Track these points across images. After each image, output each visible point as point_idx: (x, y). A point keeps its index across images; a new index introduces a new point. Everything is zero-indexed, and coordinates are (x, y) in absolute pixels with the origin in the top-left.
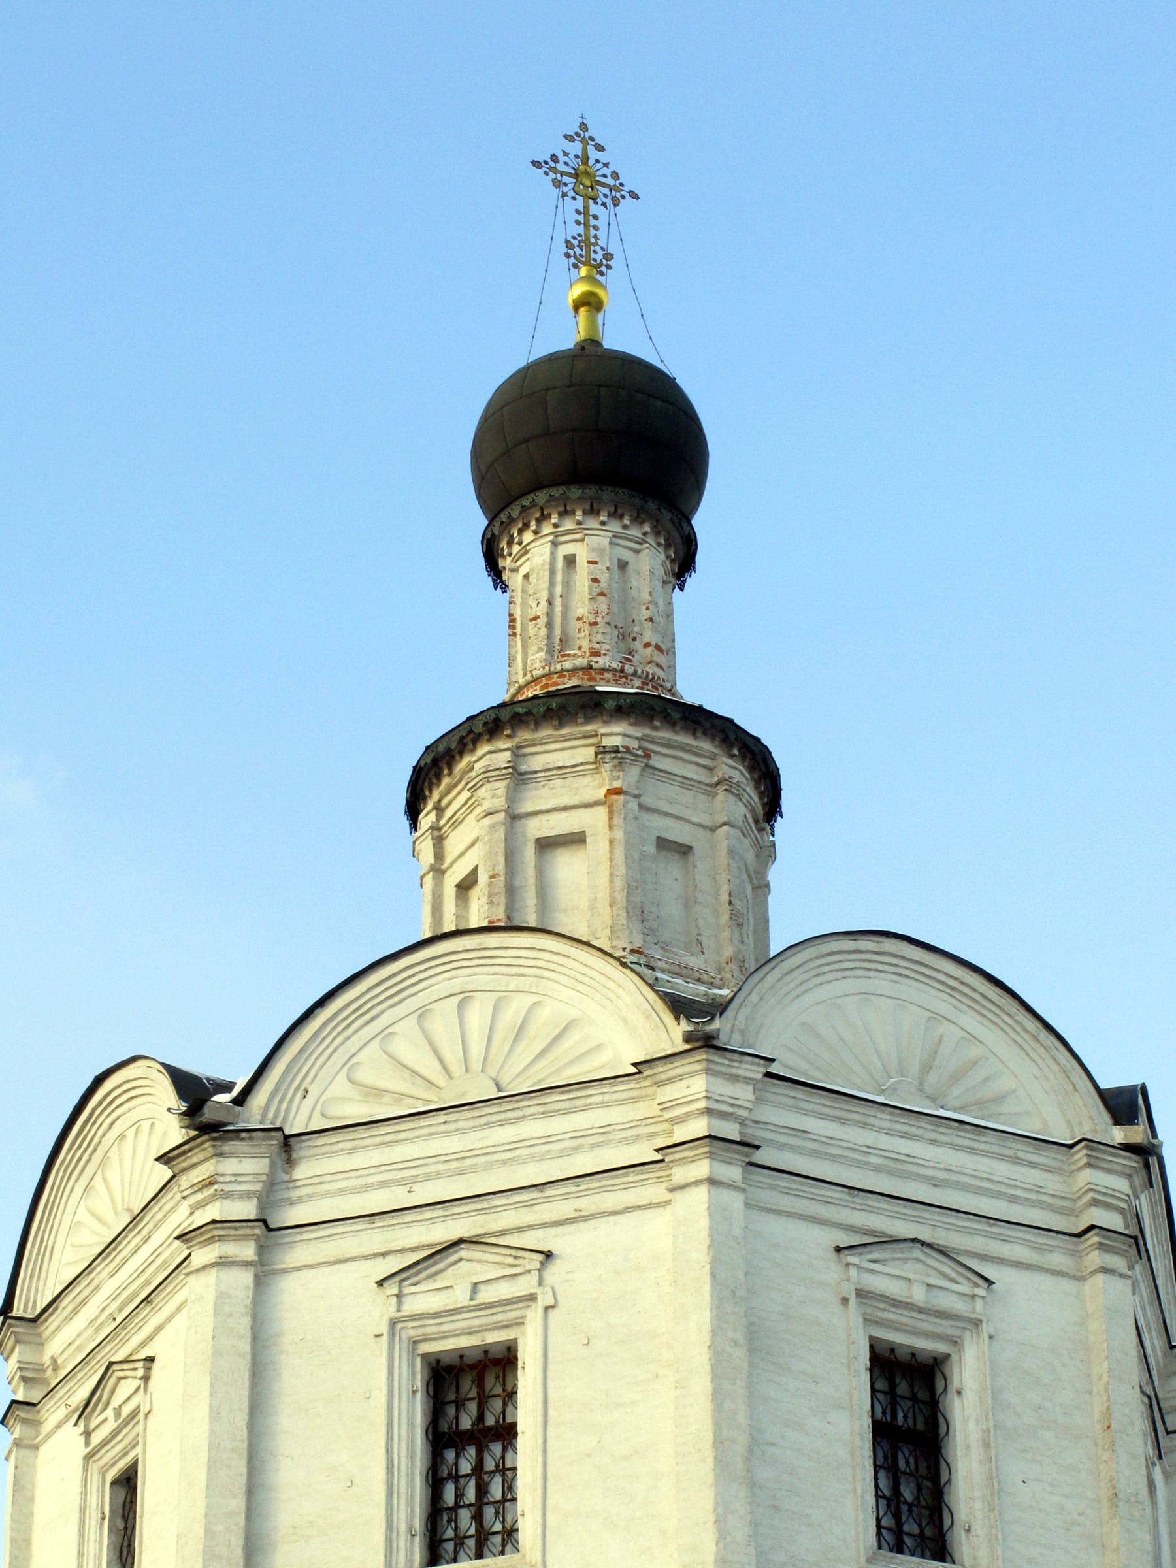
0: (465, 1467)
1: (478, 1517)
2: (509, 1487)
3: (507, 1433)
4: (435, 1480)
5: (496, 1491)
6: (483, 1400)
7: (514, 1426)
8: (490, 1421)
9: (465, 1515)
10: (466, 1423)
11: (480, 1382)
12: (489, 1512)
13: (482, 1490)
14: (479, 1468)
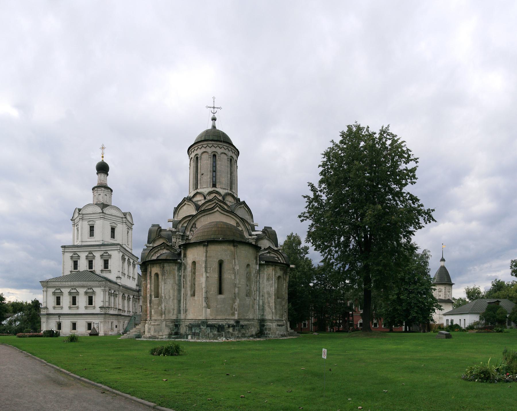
3: (94, 230)
4: (90, 232)
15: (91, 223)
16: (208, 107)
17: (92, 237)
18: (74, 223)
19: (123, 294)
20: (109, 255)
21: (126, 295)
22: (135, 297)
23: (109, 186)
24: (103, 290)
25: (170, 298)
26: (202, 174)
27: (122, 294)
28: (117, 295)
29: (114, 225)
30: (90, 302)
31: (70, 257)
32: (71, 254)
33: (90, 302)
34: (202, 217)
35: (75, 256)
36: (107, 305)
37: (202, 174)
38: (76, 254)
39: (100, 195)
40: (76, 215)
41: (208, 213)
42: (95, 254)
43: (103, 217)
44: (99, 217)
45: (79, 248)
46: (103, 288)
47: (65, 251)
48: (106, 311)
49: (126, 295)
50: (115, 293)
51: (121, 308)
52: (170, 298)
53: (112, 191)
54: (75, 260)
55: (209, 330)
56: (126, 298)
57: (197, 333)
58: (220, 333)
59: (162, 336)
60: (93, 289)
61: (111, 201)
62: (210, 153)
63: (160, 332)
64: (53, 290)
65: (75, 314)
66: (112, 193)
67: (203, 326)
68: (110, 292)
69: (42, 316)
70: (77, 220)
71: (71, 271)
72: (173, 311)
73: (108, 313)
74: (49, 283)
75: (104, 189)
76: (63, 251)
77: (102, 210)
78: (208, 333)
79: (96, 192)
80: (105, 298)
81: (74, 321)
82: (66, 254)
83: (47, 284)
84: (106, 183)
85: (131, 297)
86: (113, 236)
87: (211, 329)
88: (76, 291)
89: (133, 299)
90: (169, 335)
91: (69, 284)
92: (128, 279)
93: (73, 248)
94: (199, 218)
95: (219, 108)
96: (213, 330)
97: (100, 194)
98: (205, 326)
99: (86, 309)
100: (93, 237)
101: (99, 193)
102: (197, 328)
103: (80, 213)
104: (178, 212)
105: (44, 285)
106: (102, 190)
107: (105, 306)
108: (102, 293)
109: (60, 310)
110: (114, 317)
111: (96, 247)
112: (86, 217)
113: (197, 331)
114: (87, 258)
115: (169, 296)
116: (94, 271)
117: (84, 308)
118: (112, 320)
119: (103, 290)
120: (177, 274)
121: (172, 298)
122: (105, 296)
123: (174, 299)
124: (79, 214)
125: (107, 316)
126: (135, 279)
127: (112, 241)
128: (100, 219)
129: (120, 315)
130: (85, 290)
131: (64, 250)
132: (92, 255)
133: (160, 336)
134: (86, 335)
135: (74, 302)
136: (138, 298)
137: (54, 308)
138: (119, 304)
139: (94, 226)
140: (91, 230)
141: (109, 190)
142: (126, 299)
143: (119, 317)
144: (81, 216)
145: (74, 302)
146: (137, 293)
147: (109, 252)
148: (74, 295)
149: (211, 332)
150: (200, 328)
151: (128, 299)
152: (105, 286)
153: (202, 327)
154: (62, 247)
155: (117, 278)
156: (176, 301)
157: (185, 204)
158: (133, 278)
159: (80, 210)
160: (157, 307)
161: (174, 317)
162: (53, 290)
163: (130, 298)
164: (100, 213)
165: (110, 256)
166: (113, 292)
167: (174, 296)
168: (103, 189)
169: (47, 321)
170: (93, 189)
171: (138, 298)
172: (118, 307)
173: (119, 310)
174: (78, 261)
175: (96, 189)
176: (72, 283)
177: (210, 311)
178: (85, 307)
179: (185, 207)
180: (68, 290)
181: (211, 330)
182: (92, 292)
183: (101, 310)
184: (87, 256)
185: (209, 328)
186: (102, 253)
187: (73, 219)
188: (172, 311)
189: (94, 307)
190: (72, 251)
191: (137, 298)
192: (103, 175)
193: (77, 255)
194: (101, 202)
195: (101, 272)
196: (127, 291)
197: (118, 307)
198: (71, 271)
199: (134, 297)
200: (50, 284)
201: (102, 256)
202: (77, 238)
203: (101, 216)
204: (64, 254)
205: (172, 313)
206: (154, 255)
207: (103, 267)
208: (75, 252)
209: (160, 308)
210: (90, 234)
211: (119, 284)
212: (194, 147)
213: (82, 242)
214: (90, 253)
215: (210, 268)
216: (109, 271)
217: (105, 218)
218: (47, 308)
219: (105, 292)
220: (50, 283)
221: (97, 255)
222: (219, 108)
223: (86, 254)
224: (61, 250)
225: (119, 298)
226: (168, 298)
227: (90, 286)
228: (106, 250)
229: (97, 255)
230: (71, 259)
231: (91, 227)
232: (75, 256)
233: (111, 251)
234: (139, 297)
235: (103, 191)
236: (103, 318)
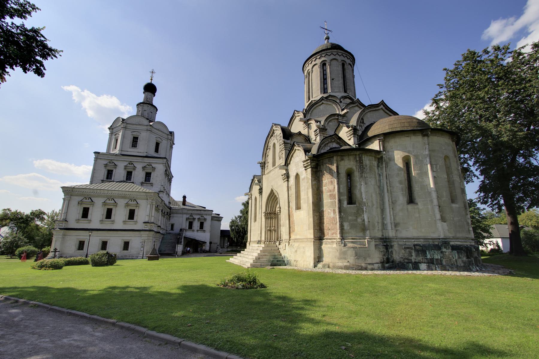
3: (137, 142)
16: (322, 28)
23: (154, 104)
25: (373, 205)
26: (333, 79)
30: (132, 215)
33: (132, 215)
34: (369, 112)
36: (152, 221)
37: (333, 79)
39: (145, 112)
41: (374, 109)
51: (159, 225)
52: (373, 205)
53: (157, 110)
55: (457, 255)
57: (437, 259)
58: (470, 260)
59: (373, 264)
62: (340, 60)
63: (368, 259)
65: (86, 229)
67: (445, 247)
72: (378, 224)
78: (456, 259)
80: (151, 211)
82: (99, 161)
86: (157, 150)
87: (458, 253)
90: (381, 262)
94: (366, 113)
95: (330, 31)
96: (461, 254)
98: (449, 248)
99: (124, 224)
101: (145, 110)
102: (436, 252)
103: (124, 122)
104: (312, 112)
107: (150, 222)
113: (437, 256)
114: (125, 169)
115: (372, 201)
117: (122, 224)
120: (377, 173)
121: (375, 206)
122: (151, 210)
123: (377, 208)
127: (156, 155)
132: (132, 166)
133: (369, 264)
135: (109, 214)
137: (78, 221)
139: (137, 138)
140: (133, 141)
141: (155, 109)
145: (109, 214)
147: (154, 165)
149: (459, 258)
150: (442, 252)
153: (444, 250)
154: (95, 153)
156: (379, 211)
157: (323, 103)
160: (355, 218)
161: (379, 235)
167: (377, 202)
174: (114, 170)
175: (142, 105)
177: (447, 226)
179: (321, 107)
181: (458, 255)
183: (146, 226)
185: (456, 251)
186: (145, 164)
188: (376, 224)
189: (137, 221)
190: (109, 159)
201: (144, 168)
203: (148, 129)
205: (377, 229)
206: (324, 148)
207: (144, 179)
209: (359, 220)
212: (321, 53)
213: (122, 151)
214: (131, 163)
215: (436, 165)
221: (139, 166)
222: (330, 31)
223: (126, 163)
225: (159, 214)
226: (371, 206)
228: (149, 163)
229: (139, 166)
231: (134, 138)
233: (155, 164)
234: (170, 214)
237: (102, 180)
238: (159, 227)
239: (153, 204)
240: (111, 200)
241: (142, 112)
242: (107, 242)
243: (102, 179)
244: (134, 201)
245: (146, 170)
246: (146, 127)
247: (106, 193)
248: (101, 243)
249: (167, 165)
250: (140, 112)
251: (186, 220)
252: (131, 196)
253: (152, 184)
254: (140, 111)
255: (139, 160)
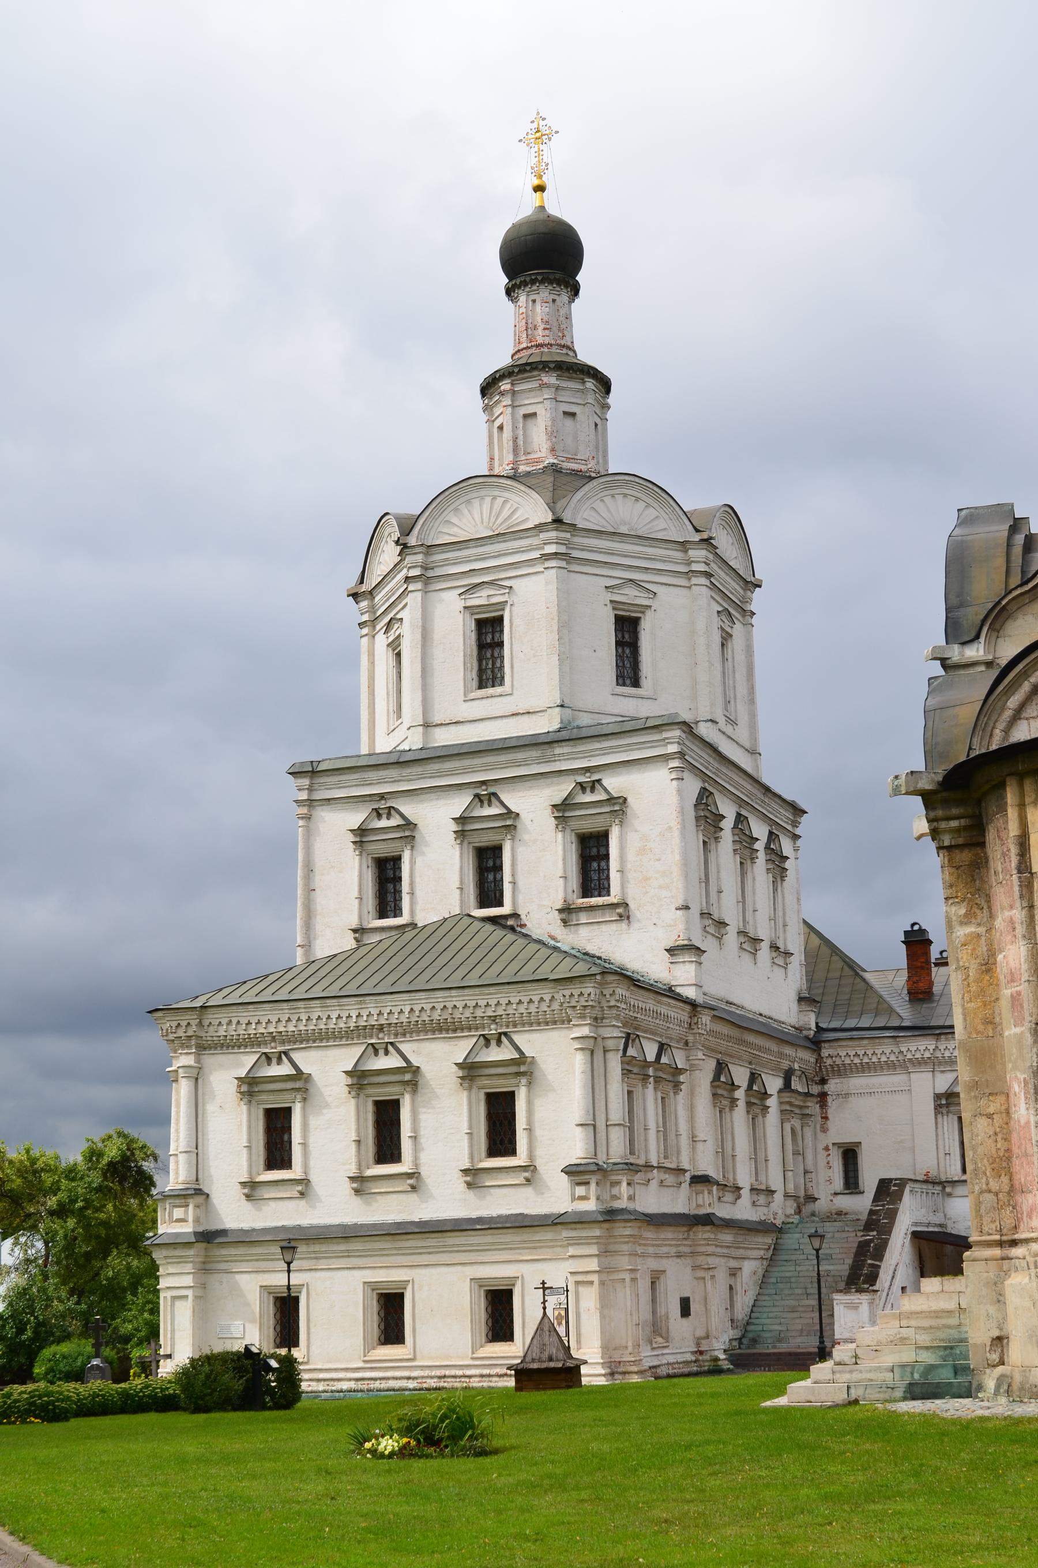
0: (489, 655)
1: (493, 672)
2: (502, 662)
3: (501, 644)
4: (480, 660)
5: (498, 665)
6: (493, 633)
7: (502, 642)
8: (496, 640)
9: (489, 672)
10: (489, 641)
11: (493, 626)
12: (496, 670)
13: (493, 664)
14: (492, 655)
15: (479, 599)
17: (490, 691)
18: (372, 609)
19: (721, 1067)
20: (611, 800)
21: (740, 1075)
22: (796, 1084)
23: (585, 355)
24: (589, 1044)
27: (712, 1064)
28: (678, 1071)
29: (631, 595)
31: (352, 838)
32: (356, 818)
35: (384, 823)
38: (390, 811)
39: (530, 422)
40: (388, 554)
42: (513, 799)
43: (563, 549)
44: (536, 554)
45: (407, 771)
46: (585, 1031)
47: (318, 795)
48: (615, 1191)
49: (740, 1075)
50: (664, 1060)
51: (707, 1165)
53: (605, 384)
54: (384, 850)
56: (740, 1094)
60: (516, 1038)
61: (601, 448)
64: (245, 1062)
66: (612, 399)
68: (631, 1052)
69: (165, 1252)
70: (392, 592)
71: (359, 931)
73: (631, 1206)
74: (211, 1017)
75: (559, 377)
76: (304, 796)
77: (552, 506)
79: (507, 401)
81: (388, 1276)
83: (200, 1024)
84: (566, 341)
85: (773, 1084)
88: (400, 1063)
89: (787, 1097)
91: (351, 1014)
92: (747, 957)
93: (373, 775)
97: (534, 415)
100: (498, 690)
101: (530, 410)
103: (412, 540)
105: (181, 1033)
106: (543, 386)
107: (601, 1159)
108: (580, 1060)
109: (291, 1205)
110: (668, 1234)
111: (520, 755)
112: (448, 563)
114: (461, 835)
116: (515, 915)
118: (657, 1256)
119: (589, 1044)
124: (405, 546)
125: (624, 1230)
126: (788, 954)
128: (539, 568)
129: (707, 1220)
130: (460, 1049)
131: (311, 789)
132: (495, 810)
134: (475, 1383)
136: (815, 1089)
138: (693, 1140)
139: (500, 619)
140: (482, 646)
141: (590, 384)
142: (741, 1104)
143: (703, 1233)
144: (419, 558)
146: (809, 1057)
147: (614, 783)
148: (386, 1093)
151: (749, 1104)
152: (596, 1012)
155: (671, 951)
158: (774, 947)
159: (407, 525)
162: (245, 1062)
163: (765, 1095)
164: (540, 528)
165: (618, 805)
166: (651, 1057)
168: (550, 379)
169: (204, 1286)
170: (488, 388)
171: (815, 1089)
172: (693, 1160)
173: (700, 1180)
176: (371, 1012)
178: (466, 1172)
180: (347, 1057)
182: (513, 1062)
183: (580, 1191)
184: (461, 820)
186: (560, 790)
187: (364, 588)
189: (530, 1168)
191: (807, 1095)
192: (544, 293)
193: (395, 821)
194: (537, 461)
195: (564, 922)
196: (742, 1042)
197: (693, 1160)
198: (359, 931)
199: (787, 1085)
200: (222, 1026)
201: (563, 810)
202: (393, 706)
203: (551, 549)
204: (308, 818)
208: (382, 797)
210: (481, 671)
211: (690, 993)
214: (485, 794)
216: (613, 906)
217: (576, 554)
218: (199, 1192)
219: (599, 1055)
220: (223, 1016)
223: (458, 804)
224: (294, 790)
225: (692, 1093)
227: (494, 1019)
228: (587, 770)
230: (359, 844)
231: (480, 624)
232: (384, 823)
233: (622, 769)
234: (823, 1081)
235: (547, 394)
236: (594, 1250)
237: (355, 931)
238: (699, 1187)
239: (605, 1051)
240: (387, 1053)
241: (515, 428)
242: (400, 1297)
243: (354, 923)
244: (499, 1042)
245: (574, 824)
246: (535, 541)
247: (354, 1014)
248: (375, 1306)
249: (699, 757)
250: (507, 433)
251: (938, 1108)
252: (479, 1013)
253: (620, 910)
254: (501, 428)
255: (525, 763)
